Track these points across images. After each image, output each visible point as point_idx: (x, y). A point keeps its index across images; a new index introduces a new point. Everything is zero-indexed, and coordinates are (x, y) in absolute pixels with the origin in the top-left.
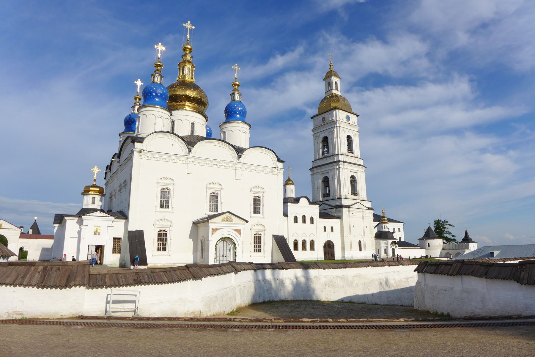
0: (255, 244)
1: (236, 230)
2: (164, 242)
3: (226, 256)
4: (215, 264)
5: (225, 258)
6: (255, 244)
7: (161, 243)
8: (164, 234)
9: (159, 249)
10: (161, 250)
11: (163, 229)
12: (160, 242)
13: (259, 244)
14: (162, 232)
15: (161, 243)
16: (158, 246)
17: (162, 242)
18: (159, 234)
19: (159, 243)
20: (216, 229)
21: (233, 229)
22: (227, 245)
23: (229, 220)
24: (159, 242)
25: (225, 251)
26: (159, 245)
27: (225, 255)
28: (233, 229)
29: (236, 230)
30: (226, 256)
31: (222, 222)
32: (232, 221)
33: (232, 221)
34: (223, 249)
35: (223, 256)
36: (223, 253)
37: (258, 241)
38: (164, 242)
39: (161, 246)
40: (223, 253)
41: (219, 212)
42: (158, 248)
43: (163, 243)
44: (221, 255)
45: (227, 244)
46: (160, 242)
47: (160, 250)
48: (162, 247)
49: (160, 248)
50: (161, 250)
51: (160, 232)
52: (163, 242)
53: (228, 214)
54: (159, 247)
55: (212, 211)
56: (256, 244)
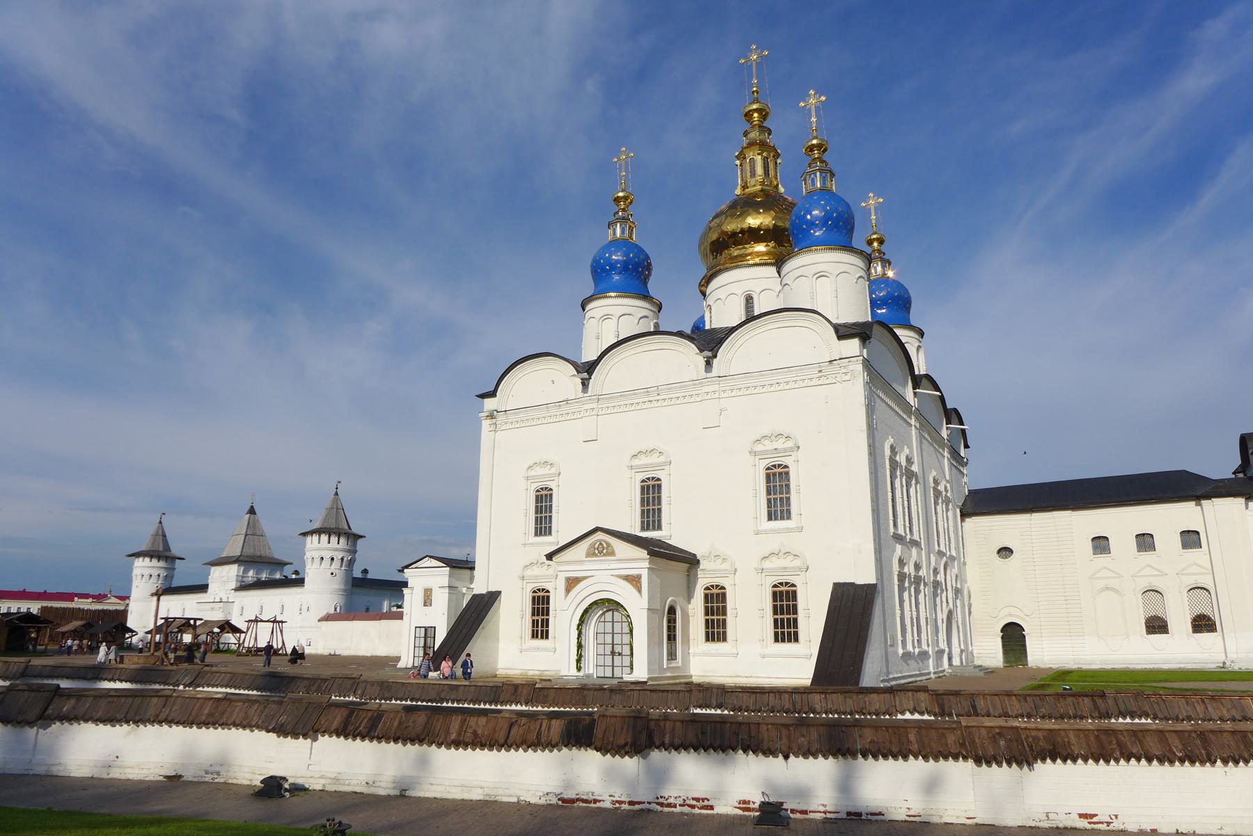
0: (776, 617)
1: (627, 578)
2: (545, 617)
3: (620, 654)
4: (581, 674)
5: (617, 659)
6: (776, 617)
7: (538, 620)
9: (534, 635)
10: (539, 637)
11: (784, 579)
12: (535, 618)
13: (792, 616)
19: (533, 621)
20: (577, 578)
22: (622, 622)
23: (605, 551)
24: (534, 618)
26: (535, 624)
27: (618, 649)
29: (627, 578)
30: (620, 654)
31: (588, 559)
32: (612, 553)
33: (612, 553)
34: (613, 634)
35: (613, 653)
36: (613, 644)
37: (718, 608)
40: (613, 644)
44: (609, 649)
45: (624, 619)
46: (535, 618)
47: (537, 637)
50: (539, 637)
51: (536, 592)
52: (542, 617)
53: (600, 536)
54: (545, 629)
56: (779, 617)
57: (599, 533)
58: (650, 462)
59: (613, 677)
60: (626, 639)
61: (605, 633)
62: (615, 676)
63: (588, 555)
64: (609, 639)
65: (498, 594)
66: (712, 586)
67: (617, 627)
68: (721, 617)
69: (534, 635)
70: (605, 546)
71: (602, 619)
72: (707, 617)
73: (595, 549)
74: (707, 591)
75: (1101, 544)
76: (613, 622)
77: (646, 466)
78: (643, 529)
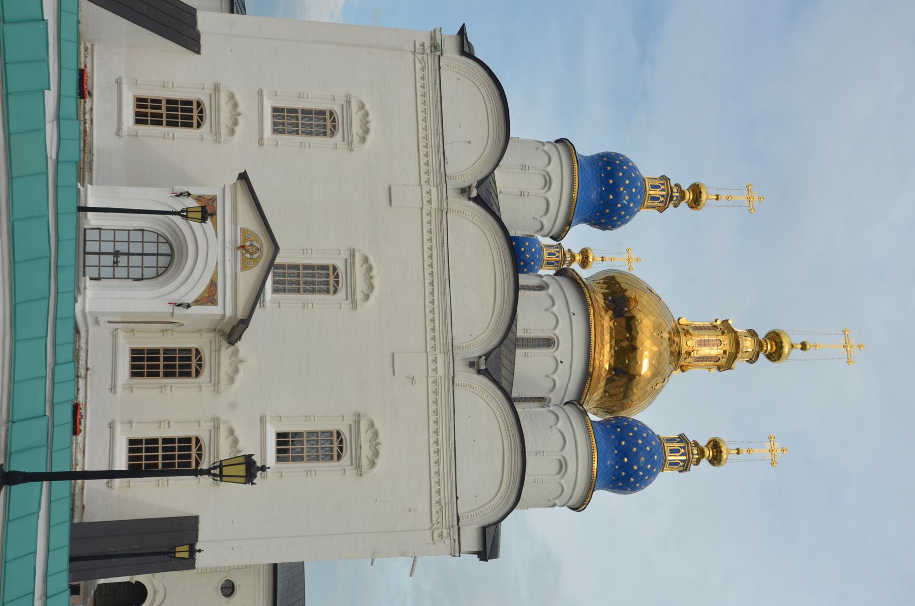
2: (164, 119)
3: (116, 263)
7: (160, 108)
8: (191, 118)
9: (141, 102)
12: (164, 105)
15: (160, 108)
16: (153, 101)
17: (163, 111)
19: (159, 101)
21: (216, 273)
23: (248, 255)
24: (164, 102)
25: (135, 260)
26: (156, 102)
27: (123, 260)
28: (216, 273)
29: (213, 284)
30: (116, 263)
32: (244, 268)
34: (143, 254)
35: (117, 254)
36: (129, 254)
39: (152, 107)
40: (129, 254)
42: (145, 100)
43: (161, 115)
45: (161, 270)
46: (164, 105)
47: (138, 106)
49: (146, 107)
59: (85, 253)
60: (136, 273)
61: (143, 242)
62: (87, 256)
63: (243, 230)
65: (198, 52)
67: (150, 261)
68: (161, 370)
69: (141, 102)
70: (255, 256)
71: (161, 240)
72: (162, 352)
73: (252, 241)
74: (194, 353)
76: (157, 255)
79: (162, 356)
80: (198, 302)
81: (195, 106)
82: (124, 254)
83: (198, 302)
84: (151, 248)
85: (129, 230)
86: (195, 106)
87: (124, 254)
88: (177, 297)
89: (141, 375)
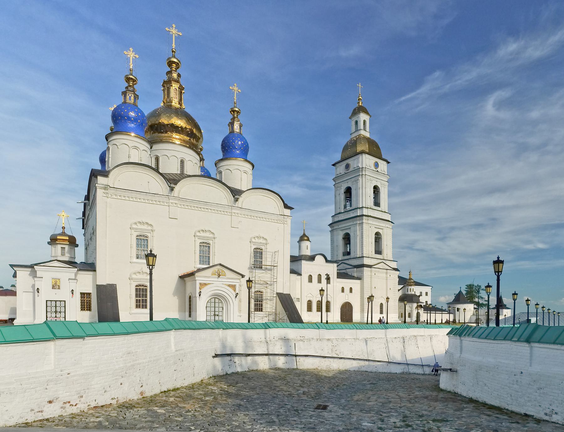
1: (229, 286)
7: (140, 300)
8: (143, 289)
12: (138, 299)
14: (140, 287)
18: (136, 289)
19: (137, 300)
25: (217, 309)
27: (217, 313)
29: (229, 286)
32: (225, 275)
33: (225, 275)
34: (215, 307)
35: (215, 315)
36: (215, 311)
38: (144, 298)
40: (215, 311)
41: (211, 265)
44: (213, 313)
45: (220, 302)
46: (138, 299)
48: (141, 304)
55: (203, 264)
57: (219, 266)
58: (205, 236)
60: (221, 309)
63: (212, 274)
64: (213, 309)
66: (257, 291)
75: (343, 290)
76: (215, 303)
77: (204, 237)
78: (200, 264)
79: (256, 303)
80: (235, 291)
81: (138, 287)
82: (215, 313)
83: (235, 291)
84: (213, 305)
85: (207, 311)
86: (138, 287)
87: (215, 313)
88: (233, 297)
89: (262, 309)
